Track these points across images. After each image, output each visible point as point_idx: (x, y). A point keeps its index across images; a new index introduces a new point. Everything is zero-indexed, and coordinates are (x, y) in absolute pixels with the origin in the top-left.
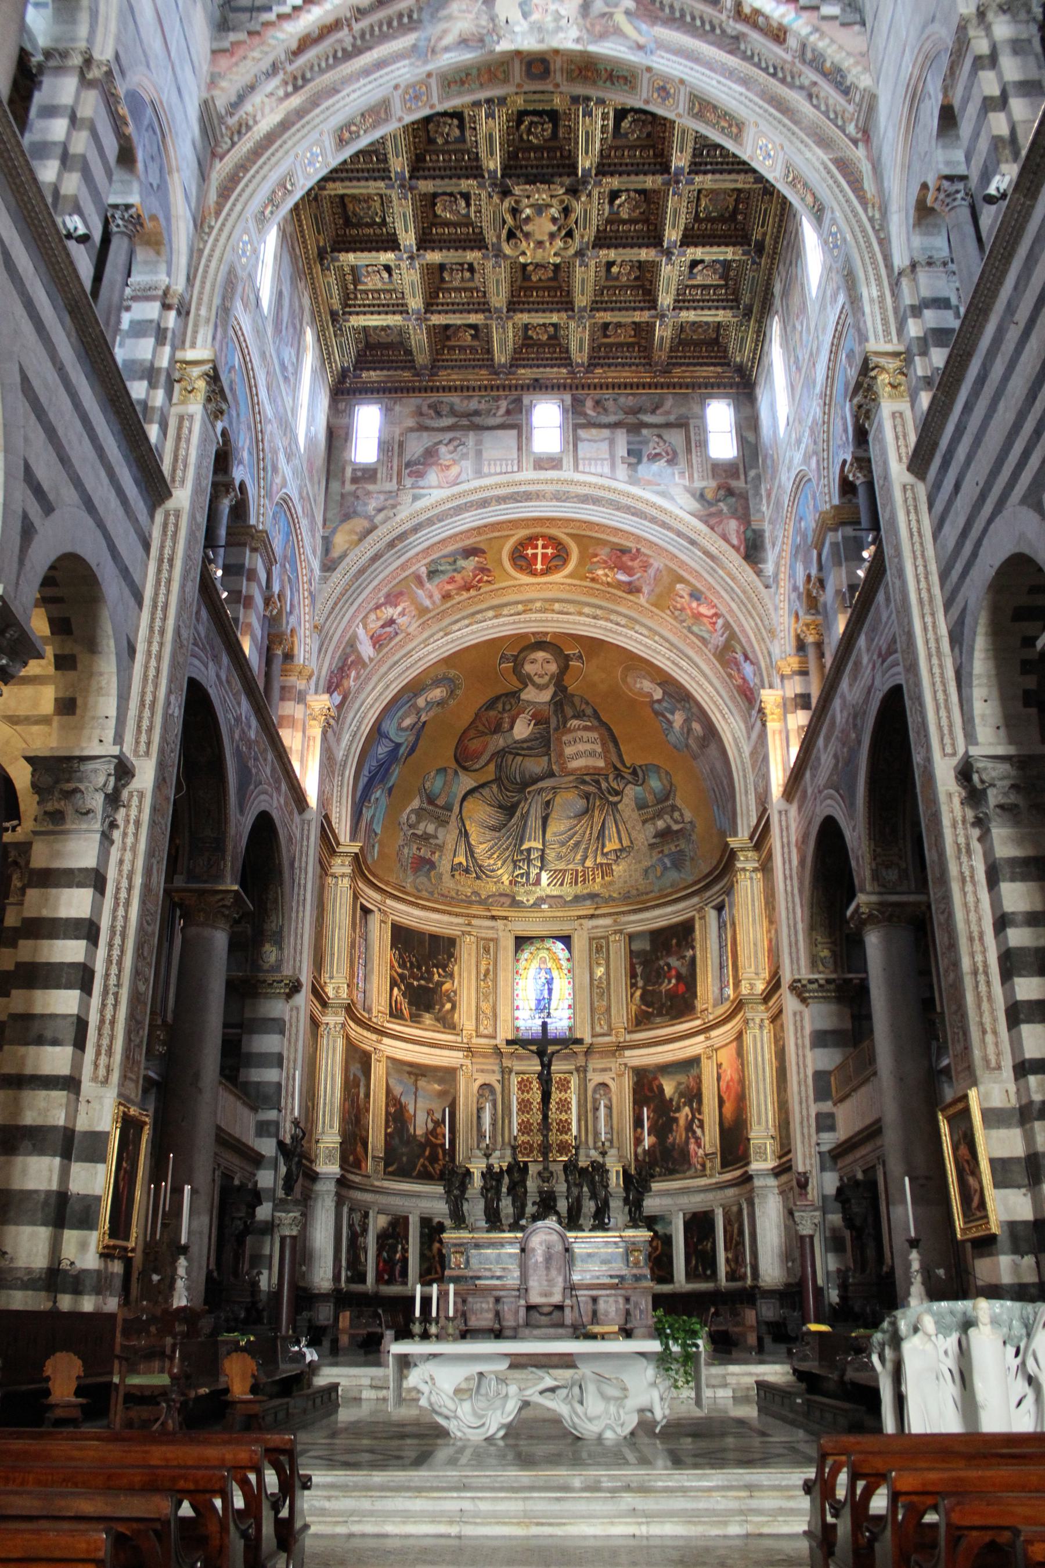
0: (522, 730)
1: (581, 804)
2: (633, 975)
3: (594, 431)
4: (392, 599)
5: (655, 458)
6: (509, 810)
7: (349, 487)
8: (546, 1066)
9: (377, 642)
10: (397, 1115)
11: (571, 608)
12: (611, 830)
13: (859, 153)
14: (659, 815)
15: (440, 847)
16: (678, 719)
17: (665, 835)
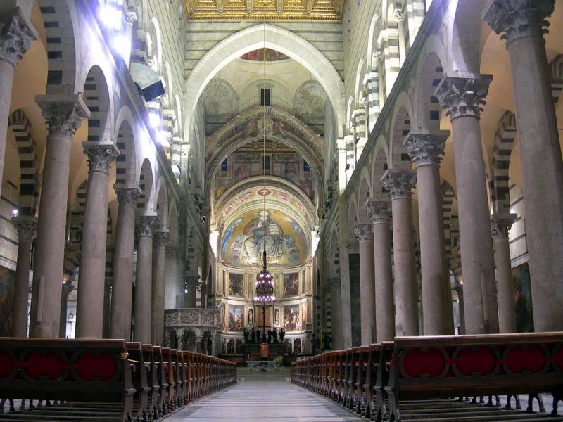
0: (259, 225)
1: (273, 242)
2: (285, 284)
3: (277, 164)
4: (230, 205)
5: (291, 171)
6: (256, 243)
7: (220, 178)
8: (264, 310)
9: (227, 213)
10: (231, 318)
11: (271, 202)
12: (280, 248)
13: (322, 164)
14: (292, 246)
15: (240, 253)
16: (296, 227)
17: (293, 251)
